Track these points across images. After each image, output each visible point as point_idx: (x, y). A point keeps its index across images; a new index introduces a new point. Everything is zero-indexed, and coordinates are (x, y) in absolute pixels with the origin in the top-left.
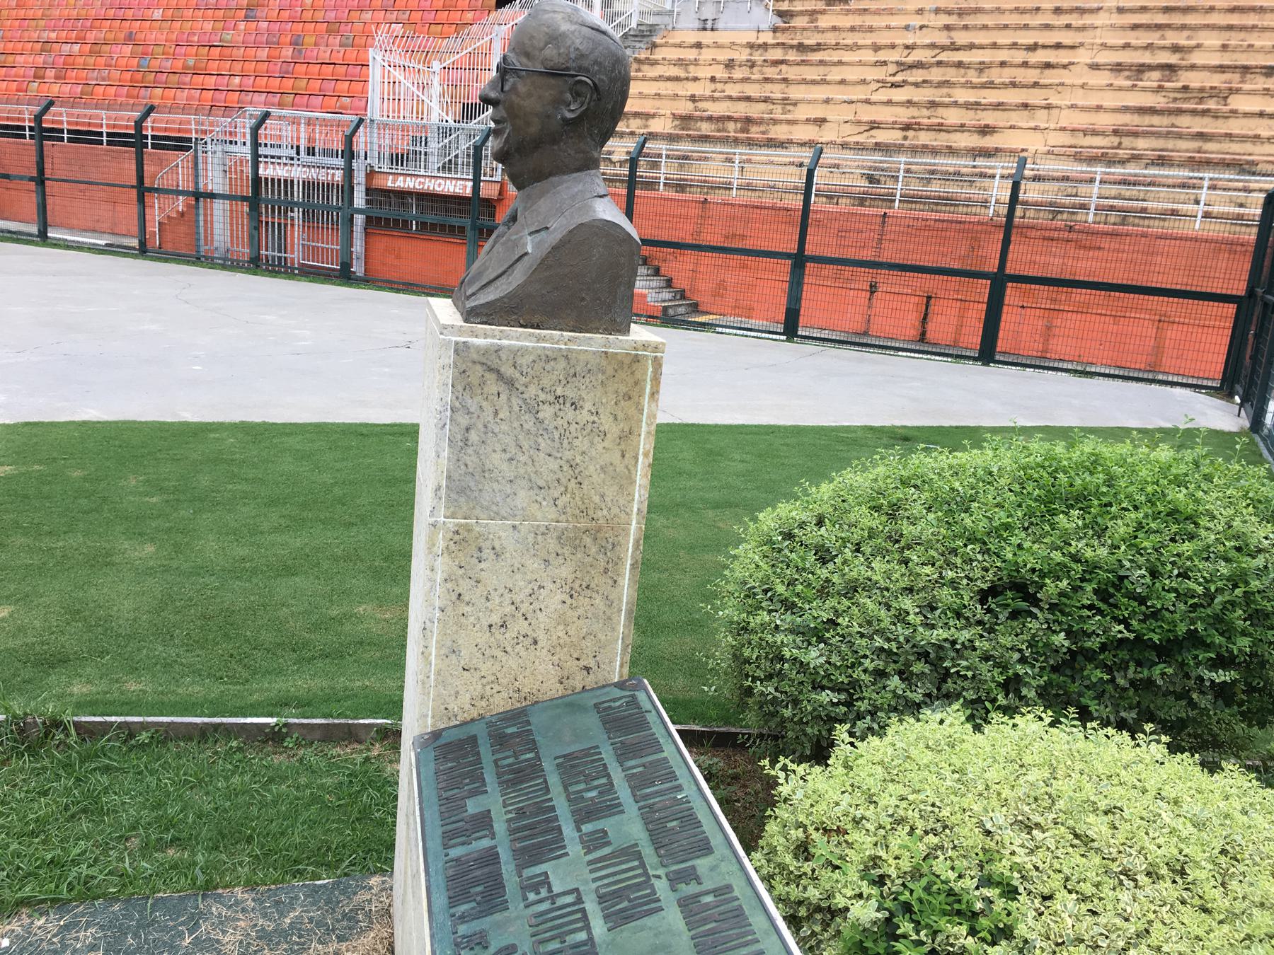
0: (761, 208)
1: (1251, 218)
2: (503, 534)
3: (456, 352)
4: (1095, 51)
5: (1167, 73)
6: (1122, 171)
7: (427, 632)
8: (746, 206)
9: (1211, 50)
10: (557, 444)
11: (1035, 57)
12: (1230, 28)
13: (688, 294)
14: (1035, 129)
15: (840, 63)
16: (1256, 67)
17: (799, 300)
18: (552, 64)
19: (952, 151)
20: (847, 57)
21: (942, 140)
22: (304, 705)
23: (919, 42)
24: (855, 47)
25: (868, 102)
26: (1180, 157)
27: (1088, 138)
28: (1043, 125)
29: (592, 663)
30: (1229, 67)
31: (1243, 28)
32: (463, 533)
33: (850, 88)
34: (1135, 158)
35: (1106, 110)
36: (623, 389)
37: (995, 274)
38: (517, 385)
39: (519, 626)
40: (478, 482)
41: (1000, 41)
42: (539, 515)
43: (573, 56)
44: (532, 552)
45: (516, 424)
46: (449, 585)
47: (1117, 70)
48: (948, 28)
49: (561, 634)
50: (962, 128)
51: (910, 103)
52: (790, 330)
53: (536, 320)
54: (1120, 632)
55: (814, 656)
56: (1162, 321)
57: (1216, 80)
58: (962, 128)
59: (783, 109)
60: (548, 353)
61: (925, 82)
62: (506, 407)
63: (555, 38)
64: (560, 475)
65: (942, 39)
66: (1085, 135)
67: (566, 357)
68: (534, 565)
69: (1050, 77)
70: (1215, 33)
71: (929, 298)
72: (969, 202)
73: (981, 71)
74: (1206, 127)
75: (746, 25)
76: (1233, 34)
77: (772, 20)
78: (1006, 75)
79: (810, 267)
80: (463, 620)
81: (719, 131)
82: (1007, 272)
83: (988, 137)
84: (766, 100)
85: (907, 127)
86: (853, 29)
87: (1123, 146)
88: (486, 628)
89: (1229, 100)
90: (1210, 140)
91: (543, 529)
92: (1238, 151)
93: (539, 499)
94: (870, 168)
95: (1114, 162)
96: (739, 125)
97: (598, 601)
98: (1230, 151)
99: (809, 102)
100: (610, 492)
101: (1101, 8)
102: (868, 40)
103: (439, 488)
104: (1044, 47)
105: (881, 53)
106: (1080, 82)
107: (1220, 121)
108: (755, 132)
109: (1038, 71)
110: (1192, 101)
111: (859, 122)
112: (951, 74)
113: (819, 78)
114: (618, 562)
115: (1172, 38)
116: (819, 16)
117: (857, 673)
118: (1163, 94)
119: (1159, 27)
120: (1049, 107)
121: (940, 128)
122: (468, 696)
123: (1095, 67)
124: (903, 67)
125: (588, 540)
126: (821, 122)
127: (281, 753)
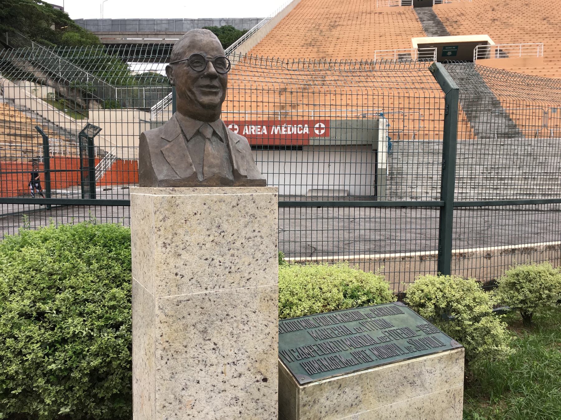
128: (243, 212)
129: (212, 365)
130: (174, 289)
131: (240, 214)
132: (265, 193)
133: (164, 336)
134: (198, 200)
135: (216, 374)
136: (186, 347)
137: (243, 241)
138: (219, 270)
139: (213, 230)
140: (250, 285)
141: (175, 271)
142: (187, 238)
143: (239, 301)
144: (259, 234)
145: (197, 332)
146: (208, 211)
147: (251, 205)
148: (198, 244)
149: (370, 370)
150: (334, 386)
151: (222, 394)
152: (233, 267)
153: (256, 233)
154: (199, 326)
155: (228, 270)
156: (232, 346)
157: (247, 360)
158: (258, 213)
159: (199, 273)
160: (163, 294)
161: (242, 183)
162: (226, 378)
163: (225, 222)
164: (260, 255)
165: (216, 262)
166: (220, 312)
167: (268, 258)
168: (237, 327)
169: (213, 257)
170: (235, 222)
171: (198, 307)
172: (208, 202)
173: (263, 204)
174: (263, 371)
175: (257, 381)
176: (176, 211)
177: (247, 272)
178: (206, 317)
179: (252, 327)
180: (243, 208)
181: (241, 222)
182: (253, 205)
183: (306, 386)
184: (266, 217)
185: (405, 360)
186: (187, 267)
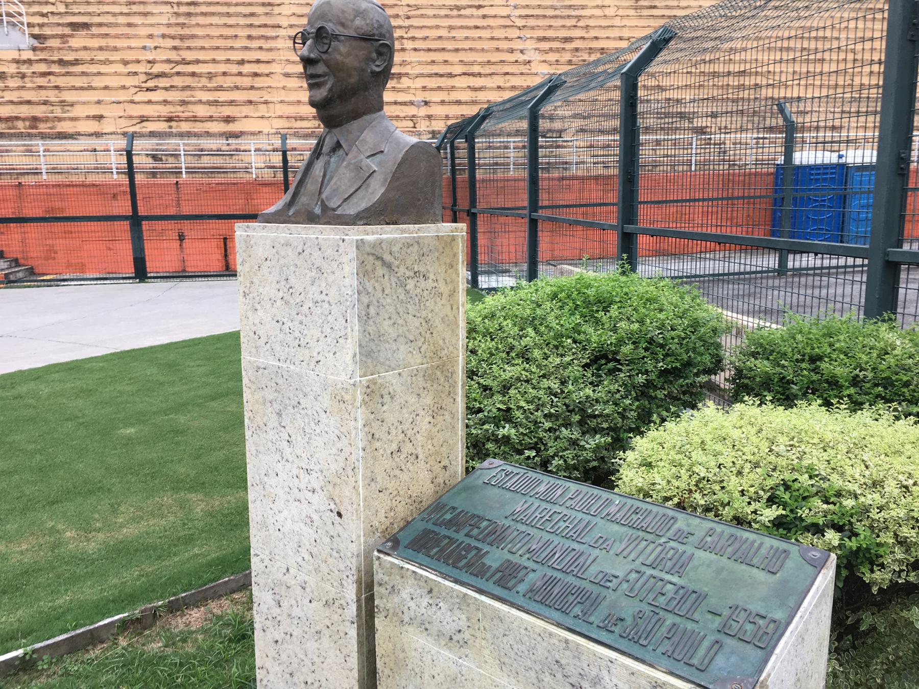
0: (73, 186)
2: (394, 381)
3: (357, 247)
7: (356, 470)
8: (59, 185)
10: (418, 307)
11: (247, 69)
13: (22, 261)
14: (262, 117)
15: (99, 74)
17: (142, 250)
19: (208, 134)
20: (104, 69)
21: (198, 127)
22: (28, 633)
23: (157, 58)
24: (107, 62)
25: (132, 102)
28: (267, 115)
29: (447, 464)
32: (372, 386)
33: (114, 92)
36: (448, 261)
39: (408, 448)
40: (377, 345)
41: (218, 58)
42: (412, 361)
43: (376, 25)
44: (411, 390)
45: (395, 297)
46: (366, 429)
48: (175, 48)
49: (430, 447)
50: (211, 118)
51: (165, 102)
52: (141, 274)
53: (394, 219)
55: (506, 430)
58: (211, 118)
59: (62, 109)
61: (172, 87)
62: (388, 285)
63: (359, 13)
64: (421, 330)
65: (174, 56)
67: (418, 243)
68: (412, 399)
69: (259, 82)
71: (225, 239)
72: (235, 171)
73: (210, 78)
75: (8, 45)
77: (29, 42)
78: (228, 82)
79: (145, 225)
80: (376, 453)
81: (10, 128)
83: (231, 124)
84: (45, 103)
85: (170, 119)
86: (101, 49)
88: (390, 456)
91: (415, 372)
93: (411, 350)
94: (153, 150)
96: (27, 123)
97: (447, 417)
99: (84, 103)
100: (447, 335)
102: (116, 56)
103: (355, 356)
104: (249, 62)
105: (129, 66)
106: (281, 85)
108: (43, 127)
109: (250, 78)
111: (131, 117)
112: (188, 81)
113: (86, 85)
114: (453, 386)
116: (69, 39)
117: (541, 434)
120: (266, 102)
121: (195, 119)
122: (383, 511)
123: (287, 75)
124: (151, 76)
125: (438, 373)
126: (99, 118)
127: (37, 677)
129: (287, 461)
130: (254, 350)
134: (268, 241)
135: (290, 474)
138: (289, 339)
141: (254, 329)
142: (261, 290)
146: (276, 256)
147: (317, 254)
149: (483, 598)
150: (421, 583)
151: (297, 503)
154: (275, 405)
156: (305, 448)
157: (319, 474)
158: (325, 266)
162: (302, 487)
164: (329, 330)
165: (286, 327)
168: (309, 423)
172: (276, 244)
173: (329, 252)
174: (337, 501)
175: (331, 511)
177: (317, 350)
181: (307, 278)
183: (382, 556)
185: (559, 625)
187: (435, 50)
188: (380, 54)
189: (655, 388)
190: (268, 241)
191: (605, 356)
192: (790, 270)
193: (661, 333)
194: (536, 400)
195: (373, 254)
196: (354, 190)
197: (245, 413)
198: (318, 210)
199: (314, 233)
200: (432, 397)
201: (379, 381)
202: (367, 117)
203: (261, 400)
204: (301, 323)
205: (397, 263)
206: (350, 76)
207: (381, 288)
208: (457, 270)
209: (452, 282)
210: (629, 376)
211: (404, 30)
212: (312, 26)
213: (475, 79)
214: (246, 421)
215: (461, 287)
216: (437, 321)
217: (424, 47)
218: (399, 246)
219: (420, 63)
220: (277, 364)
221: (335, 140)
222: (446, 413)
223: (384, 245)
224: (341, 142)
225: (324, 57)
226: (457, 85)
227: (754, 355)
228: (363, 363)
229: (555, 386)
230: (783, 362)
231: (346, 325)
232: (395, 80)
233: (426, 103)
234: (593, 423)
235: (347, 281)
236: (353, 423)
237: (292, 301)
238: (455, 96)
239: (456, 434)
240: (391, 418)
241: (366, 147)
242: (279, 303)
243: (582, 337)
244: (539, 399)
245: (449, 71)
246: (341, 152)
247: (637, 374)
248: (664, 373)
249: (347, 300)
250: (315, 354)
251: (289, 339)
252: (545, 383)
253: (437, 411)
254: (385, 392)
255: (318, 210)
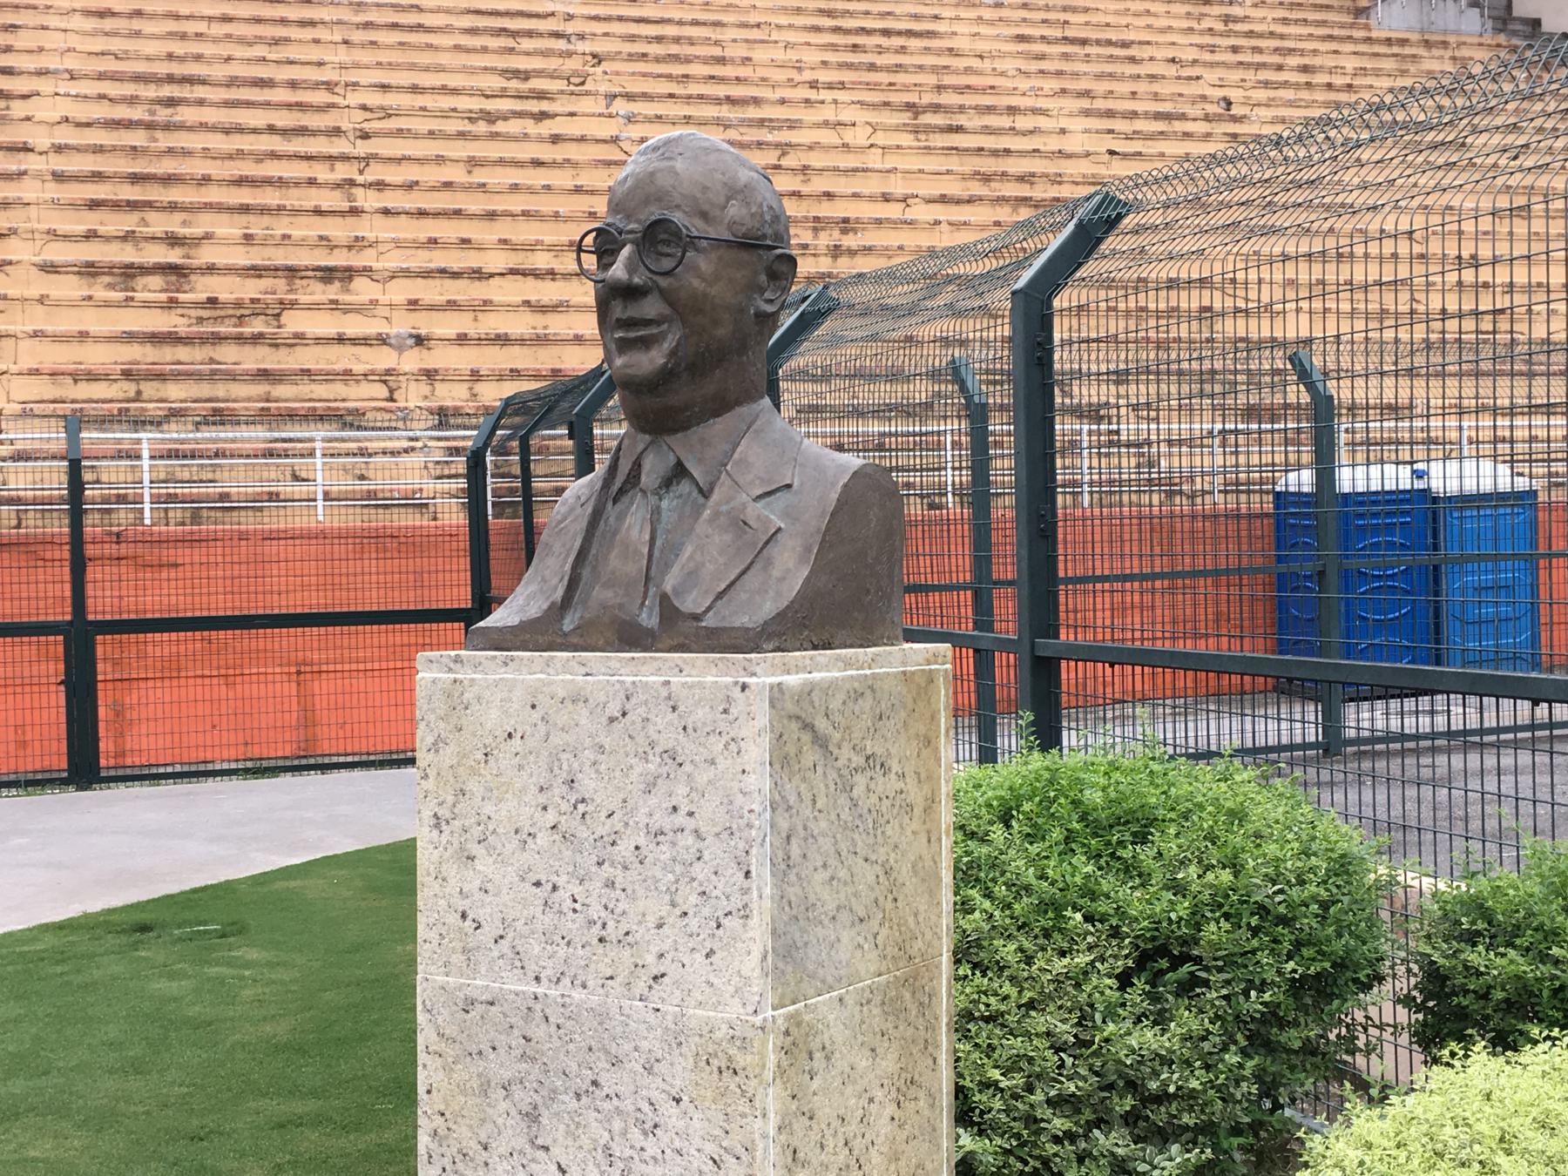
1: (388, 495)
3: (772, 705)
4: (39, 243)
5: (174, 278)
6: (160, 436)
9: (226, 242)
12: (245, 209)
16: (307, 269)
18: (744, 229)
26: (247, 409)
27: (82, 385)
30: (267, 269)
31: (264, 210)
32: (794, 1030)
34: (175, 414)
35: (98, 339)
37: (71, 623)
38: (831, 748)
40: (803, 931)
43: (768, 218)
44: (860, 1038)
45: (833, 817)
46: (783, 1138)
47: (89, 274)
54: (1295, 971)
56: (302, 672)
57: (251, 289)
60: (856, 685)
63: (736, 192)
66: (76, 381)
67: (871, 688)
70: (225, 217)
74: (263, 361)
76: (252, 218)
82: (91, 617)
87: (145, 396)
89: (284, 319)
90: (281, 381)
91: (867, 994)
92: (325, 396)
93: (861, 940)
95: (144, 422)
98: (314, 396)
101: (25, 173)
103: (765, 957)
106: (35, 293)
107: (283, 351)
110: (227, 321)
114: (932, 1028)
115: (159, 224)
118: (180, 311)
119: (133, 205)
123: (50, 268)
128: (640, 739)
130: (459, 959)
131: (630, 747)
132: (710, 679)
133: (434, 1092)
136: (486, 1149)
137: (642, 841)
138: (572, 925)
139: (556, 791)
140: (663, 1000)
141: (462, 905)
142: (489, 809)
143: (628, 1047)
144: (690, 824)
145: (513, 1112)
146: (542, 728)
148: (517, 832)
152: (611, 924)
153: (680, 819)
154: (517, 1092)
155: (596, 931)
158: (688, 748)
159: (519, 924)
160: (433, 969)
161: (681, 640)
163: (586, 768)
164: (694, 899)
166: (574, 1067)
167: (720, 913)
168: (624, 1133)
169: (554, 878)
170: (618, 773)
171: (516, 1032)
172: (542, 700)
173: (701, 715)
176: (464, 722)
177: (655, 950)
178: (536, 1071)
179: (668, 1151)
180: (639, 725)
182: (671, 716)
184: (713, 762)
186: (488, 899)
187: (437, 214)
188: (773, 276)
189: (1283, 1024)
190: (518, 693)
191: (1163, 951)
192: (1351, 742)
193: (1281, 891)
194: (1024, 1064)
195: (798, 718)
196: (738, 571)
197: (422, 1121)
198: (649, 619)
199: (658, 672)
200: (896, 1055)
201: (807, 1018)
202: (744, 410)
203: (475, 1083)
204: (610, 884)
205: (837, 736)
206: (716, 323)
207: (810, 797)
208: (937, 750)
209: (929, 778)
210: (1226, 998)
211: (355, 165)
212: (628, 217)
213: (539, 283)
214: (423, 1141)
215: (944, 790)
216: (904, 872)
217: (408, 206)
218: (841, 697)
219: (398, 244)
220: (533, 988)
221: (672, 460)
222: (921, 1094)
223: (815, 696)
224: (688, 465)
225: (663, 282)
226: (496, 298)
227: (1471, 938)
228: (778, 975)
229: (1066, 1030)
230: (1555, 951)
231: (746, 884)
232: (337, 284)
233: (420, 341)
234: (1159, 1116)
235: (752, 781)
236: (759, 1121)
237: (583, 833)
238: (493, 323)
239: (939, 1147)
240: (826, 1109)
241: (750, 477)
242: (543, 839)
243: (1103, 907)
244: (1031, 1060)
245: (475, 265)
246: (685, 487)
247: (1246, 994)
248: (1297, 986)
249: (749, 826)
250: (650, 959)
251: (572, 925)
252: (1039, 1021)
253: (907, 1086)
254: (815, 1045)
255: (649, 619)
